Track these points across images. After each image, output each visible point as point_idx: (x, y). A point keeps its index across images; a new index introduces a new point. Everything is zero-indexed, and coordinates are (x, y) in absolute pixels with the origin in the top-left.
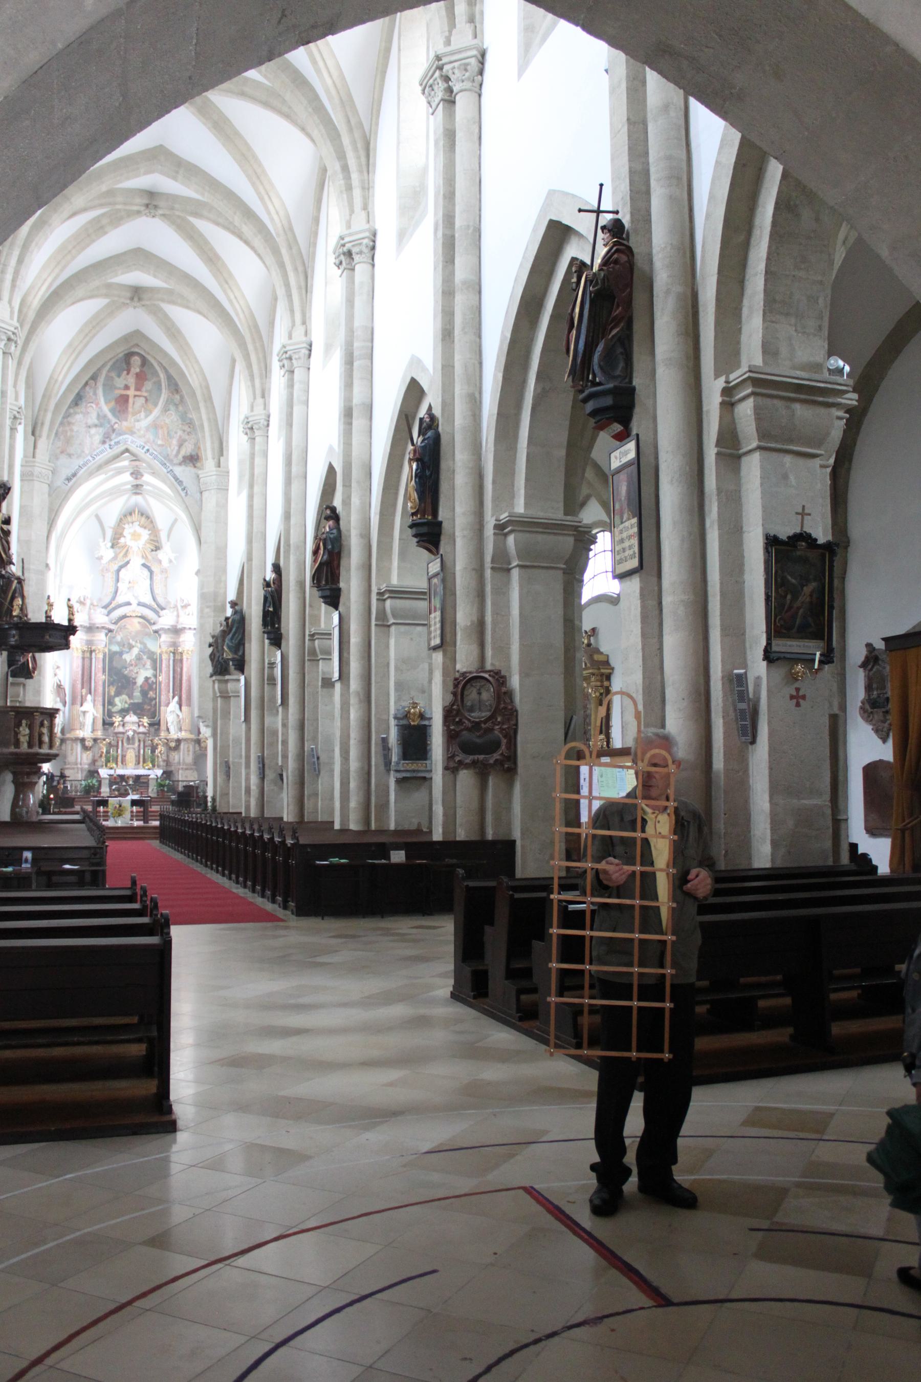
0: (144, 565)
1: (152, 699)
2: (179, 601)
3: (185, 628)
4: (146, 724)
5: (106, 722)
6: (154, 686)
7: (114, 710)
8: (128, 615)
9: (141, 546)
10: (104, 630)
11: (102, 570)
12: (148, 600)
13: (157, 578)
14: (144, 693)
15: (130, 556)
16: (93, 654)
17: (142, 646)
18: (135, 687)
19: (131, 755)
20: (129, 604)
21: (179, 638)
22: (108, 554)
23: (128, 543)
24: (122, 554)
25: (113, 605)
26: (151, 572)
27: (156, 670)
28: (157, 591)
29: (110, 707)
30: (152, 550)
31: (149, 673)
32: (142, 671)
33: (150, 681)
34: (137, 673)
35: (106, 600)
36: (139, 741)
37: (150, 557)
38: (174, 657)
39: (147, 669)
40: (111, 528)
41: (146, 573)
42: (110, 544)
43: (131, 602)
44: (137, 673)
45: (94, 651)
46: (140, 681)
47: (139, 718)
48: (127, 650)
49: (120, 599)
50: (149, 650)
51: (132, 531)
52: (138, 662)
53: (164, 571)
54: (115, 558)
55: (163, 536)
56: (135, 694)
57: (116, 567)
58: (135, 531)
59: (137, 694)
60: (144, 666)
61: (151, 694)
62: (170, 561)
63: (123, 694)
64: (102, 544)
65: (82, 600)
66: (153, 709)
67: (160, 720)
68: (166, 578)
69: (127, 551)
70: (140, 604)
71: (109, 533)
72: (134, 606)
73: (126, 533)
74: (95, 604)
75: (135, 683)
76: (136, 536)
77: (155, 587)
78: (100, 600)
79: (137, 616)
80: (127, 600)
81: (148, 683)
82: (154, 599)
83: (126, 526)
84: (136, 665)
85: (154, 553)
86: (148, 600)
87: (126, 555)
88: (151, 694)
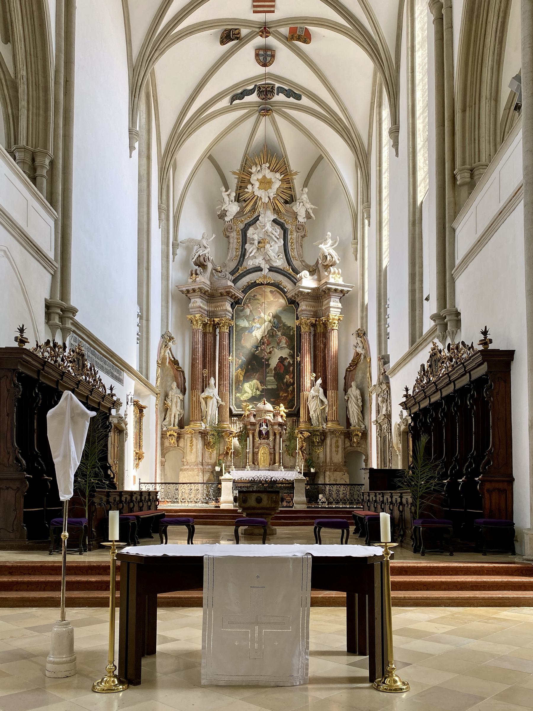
0: (275, 221)
1: (288, 385)
2: (320, 262)
3: (329, 289)
4: (282, 413)
5: (234, 412)
6: (291, 369)
7: (244, 397)
8: (257, 282)
9: (272, 195)
10: (229, 298)
11: (226, 230)
12: (280, 262)
13: (293, 236)
14: (279, 377)
15: (261, 210)
16: (218, 330)
17: (275, 320)
18: (267, 370)
19: (263, 454)
20: (259, 269)
21: (322, 306)
22: (233, 209)
23: (258, 193)
24: (248, 208)
25: (240, 272)
26: (285, 231)
27: (292, 349)
28: (293, 253)
29: (238, 395)
30: (286, 202)
31: (284, 353)
32: (275, 349)
33: (286, 363)
34: (270, 353)
35: (232, 265)
36: (275, 434)
37: (282, 210)
38: (315, 331)
39: (282, 348)
40: (234, 173)
41: (278, 231)
42: (234, 194)
43: (262, 266)
44: (270, 353)
45: (218, 324)
46: (274, 362)
47: (274, 408)
48: (258, 326)
49: (250, 263)
50: (284, 325)
51: (260, 176)
52: (270, 339)
53: (300, 228)
54: (240, 213)
55: (298, 182)
56: (267, 378)
57: (242, 226)
58: (264, 177)
59: (270, 378)
60: (278, 344)
61: (288, 378)
62: (308, 216)
63: (254, 378)
64: (225, 195)
65: (202, 259)
66: (290, 397)
67: (299, 409)
68: (303, 237)
69: (256, 203)
70: (272, 269)
71: (233, 182)
72: (266, 271)
73: (254, 179)
74: (219, 268)
75: (268, 365)
76: (266, 183)
77: (290, 248)
78: (224, 266)
79: (268, 284)
80: (257, 265)
81: (284, 365)
82: (289, 263)
83: (254, 170)
84: (268, 345)
85: (288, 205)
86: (280, 262)
87: (254, 209)
88: (288, 378)
